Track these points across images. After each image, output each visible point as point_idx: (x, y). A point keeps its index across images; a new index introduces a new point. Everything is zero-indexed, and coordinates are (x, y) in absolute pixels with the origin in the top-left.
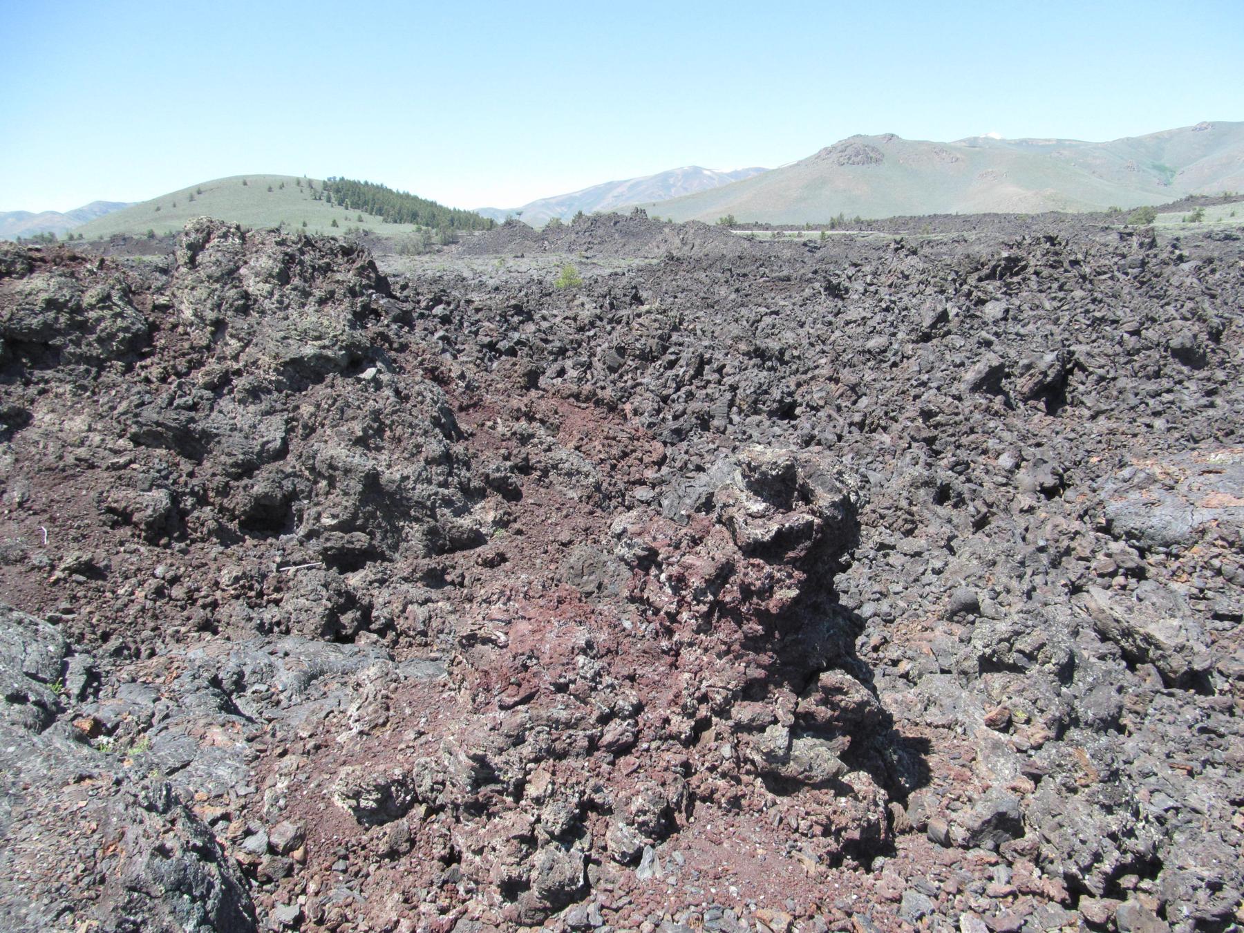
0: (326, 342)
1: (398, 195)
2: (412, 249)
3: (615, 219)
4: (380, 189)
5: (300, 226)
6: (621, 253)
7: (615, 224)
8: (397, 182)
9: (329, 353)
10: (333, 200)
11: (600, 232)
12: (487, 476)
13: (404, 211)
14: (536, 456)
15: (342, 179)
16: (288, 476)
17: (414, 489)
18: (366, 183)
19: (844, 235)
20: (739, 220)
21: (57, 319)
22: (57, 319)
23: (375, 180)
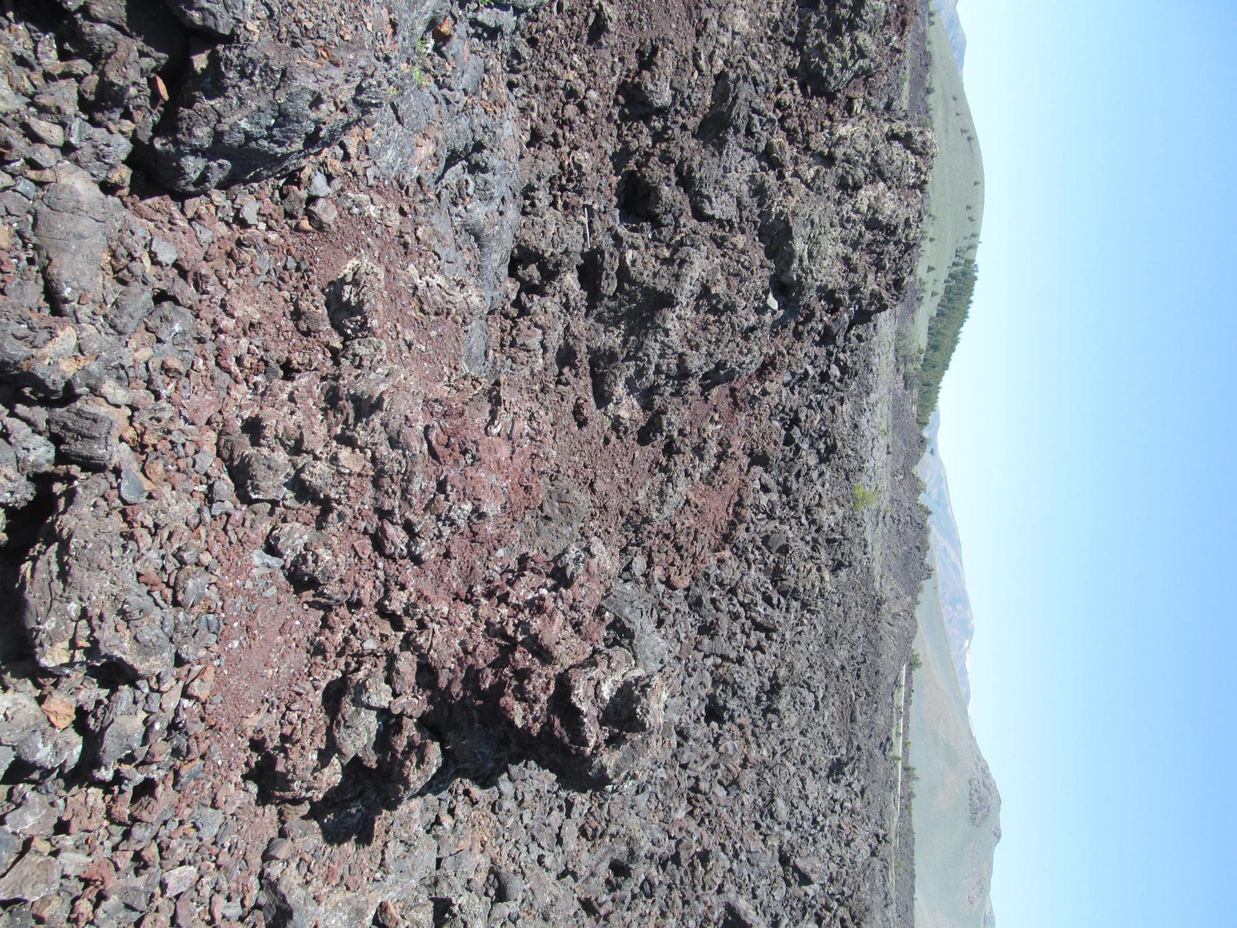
0: (806, 263)
1: (957, 333)
2: (901, 344)
3: (922, 547)
4: (964, 316)
5: (930, 235)
7: (918, 548)
8: (969, 333)
9: (795, 265)
10: (955, 268)
12: (665, 413)
13: (940, 338)
14: (682, 462)
15: (975, 278)
16: (676, 220)
17: (656, 341)
18: (971, 302)
19: (896, 780)
20: (916, 673)
21: (845, 6)
22: (845, 6)
23: (973, 311)
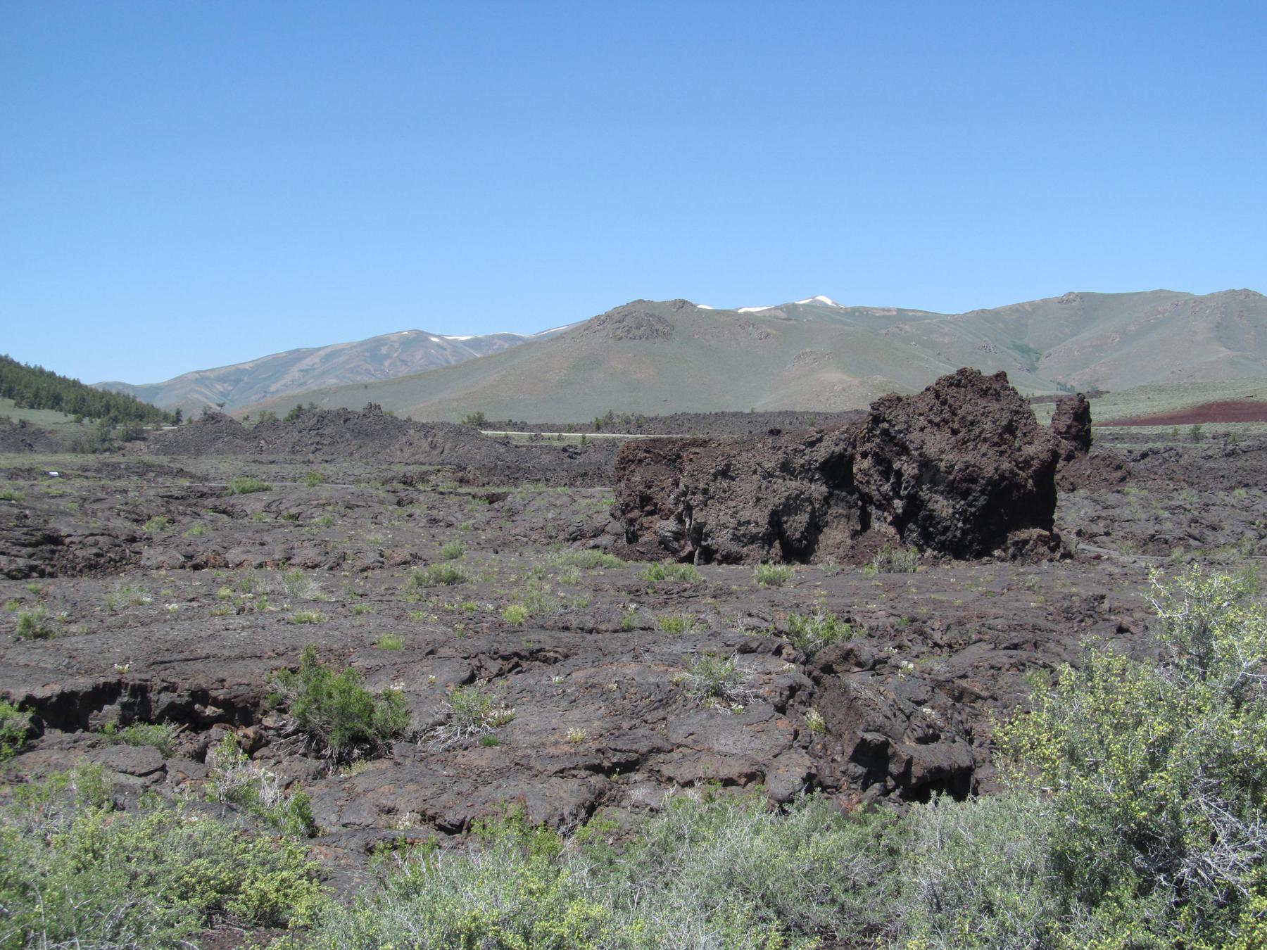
1: (27, 370)
2: (87, 446)
3: (345, 416)
6: (357, 456)
7: (345, 421)
11: (328, 431)
19: (606, 440)
20: (489, 418)
